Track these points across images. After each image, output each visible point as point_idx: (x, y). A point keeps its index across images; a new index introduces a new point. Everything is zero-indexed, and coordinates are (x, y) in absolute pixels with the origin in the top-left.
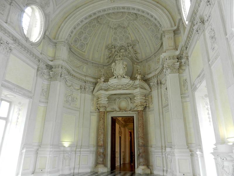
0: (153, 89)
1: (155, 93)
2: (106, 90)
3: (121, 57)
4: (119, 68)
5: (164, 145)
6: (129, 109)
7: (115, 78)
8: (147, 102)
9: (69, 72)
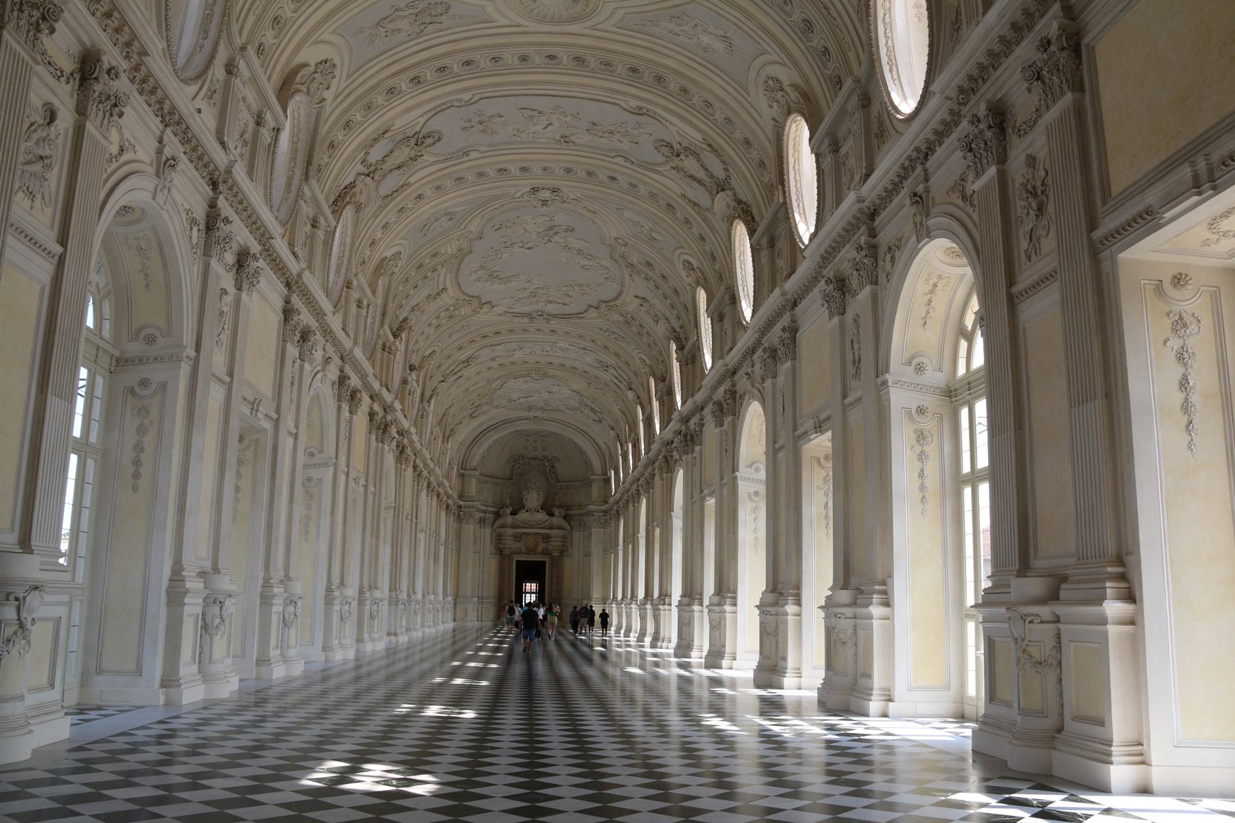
1: (576, 534)
2: (512, 527)
4: (533, 499)
6: (540, 549)
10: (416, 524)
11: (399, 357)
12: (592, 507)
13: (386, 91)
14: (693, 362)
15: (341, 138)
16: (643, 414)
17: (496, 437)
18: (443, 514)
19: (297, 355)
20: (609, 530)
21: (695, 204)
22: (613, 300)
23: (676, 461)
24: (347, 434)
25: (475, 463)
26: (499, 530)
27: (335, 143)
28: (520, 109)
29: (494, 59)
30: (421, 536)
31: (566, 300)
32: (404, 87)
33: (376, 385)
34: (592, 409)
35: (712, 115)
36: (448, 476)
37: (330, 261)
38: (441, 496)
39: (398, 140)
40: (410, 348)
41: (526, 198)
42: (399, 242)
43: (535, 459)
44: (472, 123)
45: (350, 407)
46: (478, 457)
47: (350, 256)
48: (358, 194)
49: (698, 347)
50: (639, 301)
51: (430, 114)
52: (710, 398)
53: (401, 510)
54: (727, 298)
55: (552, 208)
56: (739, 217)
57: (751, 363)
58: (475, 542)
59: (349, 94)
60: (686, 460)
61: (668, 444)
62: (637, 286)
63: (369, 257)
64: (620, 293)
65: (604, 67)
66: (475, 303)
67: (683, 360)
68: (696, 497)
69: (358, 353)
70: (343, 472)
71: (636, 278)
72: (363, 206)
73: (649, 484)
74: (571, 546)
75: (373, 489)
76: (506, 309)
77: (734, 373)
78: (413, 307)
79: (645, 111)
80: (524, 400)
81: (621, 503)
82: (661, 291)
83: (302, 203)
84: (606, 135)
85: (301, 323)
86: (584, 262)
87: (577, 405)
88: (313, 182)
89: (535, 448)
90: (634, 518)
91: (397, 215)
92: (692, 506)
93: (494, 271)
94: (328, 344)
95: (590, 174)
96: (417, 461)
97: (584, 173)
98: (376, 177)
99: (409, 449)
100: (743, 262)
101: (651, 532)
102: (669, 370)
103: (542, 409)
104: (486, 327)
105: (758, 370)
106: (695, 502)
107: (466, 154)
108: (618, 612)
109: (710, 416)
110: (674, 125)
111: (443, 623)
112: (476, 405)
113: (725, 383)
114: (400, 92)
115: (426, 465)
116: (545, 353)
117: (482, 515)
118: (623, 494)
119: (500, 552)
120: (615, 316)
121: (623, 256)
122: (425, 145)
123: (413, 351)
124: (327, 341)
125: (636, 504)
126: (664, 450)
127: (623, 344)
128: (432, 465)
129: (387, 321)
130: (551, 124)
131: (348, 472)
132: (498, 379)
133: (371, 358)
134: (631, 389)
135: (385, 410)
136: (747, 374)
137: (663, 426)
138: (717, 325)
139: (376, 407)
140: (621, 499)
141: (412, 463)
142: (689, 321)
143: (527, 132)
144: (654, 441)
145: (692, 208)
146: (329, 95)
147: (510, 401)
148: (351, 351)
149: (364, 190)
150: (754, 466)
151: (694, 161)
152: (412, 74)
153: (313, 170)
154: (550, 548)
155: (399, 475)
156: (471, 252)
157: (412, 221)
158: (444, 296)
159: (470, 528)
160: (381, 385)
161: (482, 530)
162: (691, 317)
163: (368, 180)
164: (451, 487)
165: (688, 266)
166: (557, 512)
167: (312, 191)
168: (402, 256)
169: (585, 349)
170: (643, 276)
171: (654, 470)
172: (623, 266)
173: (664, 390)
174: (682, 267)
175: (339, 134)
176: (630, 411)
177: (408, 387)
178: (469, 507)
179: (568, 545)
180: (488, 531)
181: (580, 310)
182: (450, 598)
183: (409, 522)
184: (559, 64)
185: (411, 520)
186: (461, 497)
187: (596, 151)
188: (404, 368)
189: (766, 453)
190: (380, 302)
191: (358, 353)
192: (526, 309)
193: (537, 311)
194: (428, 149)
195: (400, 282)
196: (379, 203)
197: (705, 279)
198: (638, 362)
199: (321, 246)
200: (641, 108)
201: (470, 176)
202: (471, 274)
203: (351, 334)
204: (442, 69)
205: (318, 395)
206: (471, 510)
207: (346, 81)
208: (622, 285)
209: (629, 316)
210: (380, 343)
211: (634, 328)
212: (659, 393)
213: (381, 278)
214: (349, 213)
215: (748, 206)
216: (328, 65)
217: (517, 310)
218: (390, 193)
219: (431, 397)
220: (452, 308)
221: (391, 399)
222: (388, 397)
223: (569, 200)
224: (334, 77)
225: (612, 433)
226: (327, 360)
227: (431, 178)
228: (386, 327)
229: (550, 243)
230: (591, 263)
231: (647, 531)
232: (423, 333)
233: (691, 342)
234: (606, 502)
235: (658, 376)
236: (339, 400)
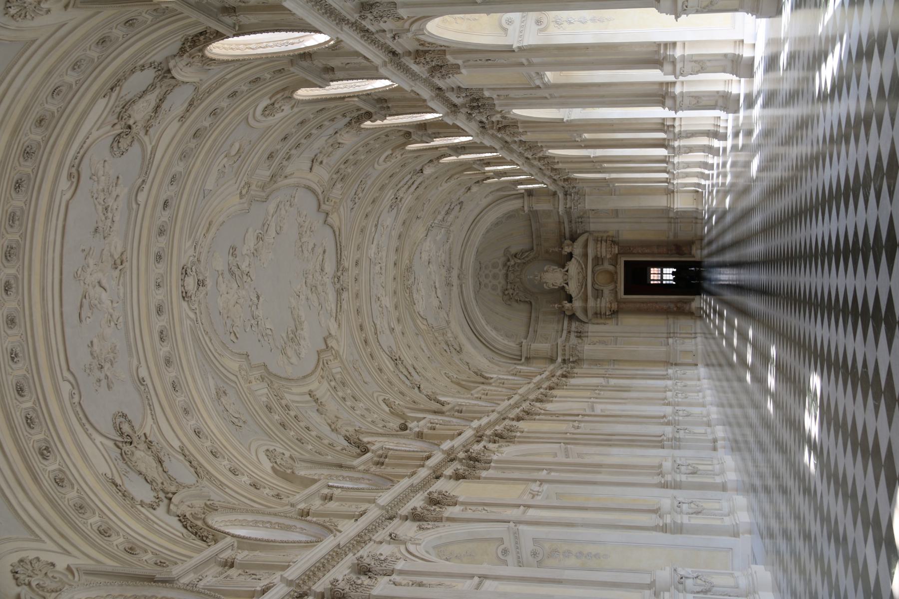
0: (588, 230)
1: (592, 227)
2: (586, 300)
4: (553, 277)
5: (666, 220)
6: (611, 268)
7: (567, 284)
10: (584, 415)
11: (391, 444)
12: (561, 209)
13: (60, 489)
14: (386, 101)
15: (121, 540)
16: (450, 156)
17: (483, 322)
18: (573, 381)
19: (387, 578)
20: (587, 190)
21: (190, 105)
22: (317, 197)
23: (504, 118)
24: (480, 508)
25: (513, 345)
26: (590, 313)
27: (128, 546)
28: (81, 321)
29: (13, 359)
30: (599, 409)
31: (320, 250)
32: (55, 466)
33: (423, 473)
34: (447, 213)
35: (71, 86)
36: (529, 377)
37: (274, 541)
38: (552, 385)
39: (125, 466)
40: (380, 431)
41: (196, 306)
42: (254, 454)
43: (507, 276)
44: (102, 376)
45: (449, 505)
46: (506, 342)
47: (269, 514)
48: (193, 511)
49: (367, 96)
50: (316, 167)
51: (91, 430)
52: (425, 81)
53: (568, 435)
54: (304, 64)
55: (207, 274)
56: (201, 50)
57: (383, 34)
58: (604, 343)
59: (62, 536)
60: (501, 106)
61: (483, 127)
62: (298, 167)
63: (271, 489)
64: (308, 188)
65: (17, 222)
66: (326, 356)
67: (383, 112)
68: (545, 93)
69: (385, 498)
70: (524, 512)
71: (288, 171)
72: (208, 503)
73: (531, 146)
74: (608, 232)
75: (545, 472)
76: (333, 320)
77: (394, 53)
78: (333, 430)
79: (74, 170)
80: (439, 291)
81: (555, 177)
82: (303, 141)
83: (201, 584)
84: (110, 215)
85: (347, 577)
86: (272, 232)
87: (443, 230)
88: (175, 571)
89: (495, 277)
90: (572, 162)
91: (220, 459)
92: (555, 97)
93: (288, 337)
94: (373, 538)
95: (161, 232)
96: (511, 416)
97: (160, 239)
98: (173, 489)
99: (497, 427)
100: (259, 45)
101: (590, 143)
102: (396, 128)
103: (449, 270)
104: (354, 343)
105: (389, 25)
106: (550, 95)
107: (142, 381)
108: (683, 177)
109: (448, 80)
110: (90, 133)
111: (699, 380)
112: (446, 348)
113: (407, 64)
114: (61, 470)
115: (516, 405)
116: (383, 271)
117: (573, 335)
118: (545, 175)
119: (614, 313)
120: (336, 192)
121: (263, 187)
122: (130, 432)
123: (385, 427)
124: (370, 539)
125: (556, 161)
126: (490, 132)
127: (369, 182)
128: (517, 397)
129: (349, 462)
130: (99, 282)
131: (525, 506)
132: (416, 325)
133: (391, 480)
134: (422, 171)
135: (452, 460)
136: (394, 38)
137: (462, 133)
138: (338, 74)
139: (449, 471)
140: (550, 177)
141: (514, 423)
142: (336, 107)
143: (111, 311)
144: (481, 143)
145: (196, 108)
146: (62, 562)
147: (440, 308)
148: (383, 508)
149: (188, 503)
150: (505, 26)
151: (135, 107)
152: (36, 460)
153: (161, 573)
154: (609, 256)
155: (527, 439)
156: (265, 366)
157: (228, 440)
158: (318, 394)
159: (588, 349)
160: (423, 466)
161: (590, 334)
162: (332, 104)
163: (176, 499)
164: (542, 372)
165: (269, 110)
166: (567, 250)
167: (187, 573)
168: (271, 448)
169: (376, 226)
170: (285, 163)
171: (515, 142)
172: (275, 186)
173: (420, 133)
174: (271, 118)
175: (115, 543)
176: (448, 171)
177: (425, 430)
178: (564, 350)
179: (605, 235)
180: (591, 328)
181: (329, 231)
182: (670, 371)
183: (582, 425)
184: (16, 277)
185: (580, 421)
186: (552, 360)
187: (132, 227)
188: (404, 437)
189: (488, 13)
190: (325, 472)
191: (385, 498)
192: (331, 296)
193: (334, 283)
194: (136, 428)
195: (301, 448)
196: (205, 482)
197: (284, 90)
198: (389, 164)
199: (256, 553)
200: (70, 175)
201: (171, 374)
202: (292, 364)
203: (364, 506)
204: (29, 422)
205: (434, 548)
206: (567, 348)
207: (43, 542)
208: (297, 186)
209: (335, 176)
210: (374, 469)
211: (350, 170)
212: (424, 139)
213: (297, 473)
214: (216, 519)
215: (187, 39)
216: (19, 570)
217: (333, 306)
218: (192, 470)
219: (438, 402)
220: (333, 383)
221: (440, 453)
222: (437, 458)
223: (196, 254)
224: (38, 559)
225: (475, 189)
226: (393, 538)
227: (174, 422)
228: (356, 462)
229: (251, 274)
230: (273, 224)
231: (587, 147)
232: (363, 416)
233: (361, 105)
234: (555, 194)
235: (403, 140)
236: (440, 520)
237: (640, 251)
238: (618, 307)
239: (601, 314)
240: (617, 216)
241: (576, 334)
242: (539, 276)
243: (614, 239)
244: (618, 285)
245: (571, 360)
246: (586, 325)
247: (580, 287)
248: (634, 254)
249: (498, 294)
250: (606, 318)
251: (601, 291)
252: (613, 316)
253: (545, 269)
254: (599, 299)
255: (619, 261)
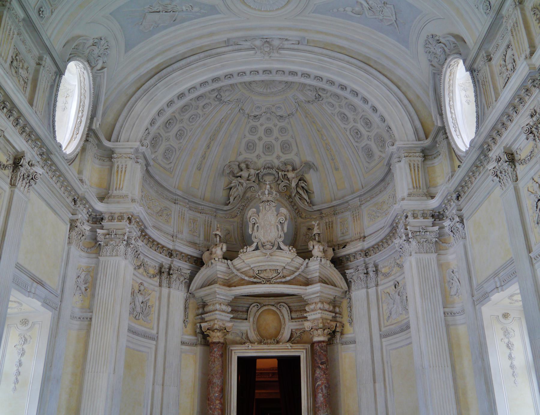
0: (353, 287)
2: (229, 284)
3: (274, 194)
7: (257, 248)
8: (338, 319)
9: (144, 235)
74: (351, 322)
117: (165, 260)
161: (165, 290)
179: (345, 320)
237: (319, 383)
238: (214, 343)
239: (202, 314)
240: (383, 336)
241: (167, 266)
242: (270, 198)
243: (338, 335)
244: (256, 346)
245: (99, 231)
246: (183, 287)
247: (251, 273)
248: (314, 372)
249: (240, 154)
250: (195, 324)
251: (245, 316)
252: (200, 336)
253: (283, 210)
254: (229, 309)
255: (299, 346)
